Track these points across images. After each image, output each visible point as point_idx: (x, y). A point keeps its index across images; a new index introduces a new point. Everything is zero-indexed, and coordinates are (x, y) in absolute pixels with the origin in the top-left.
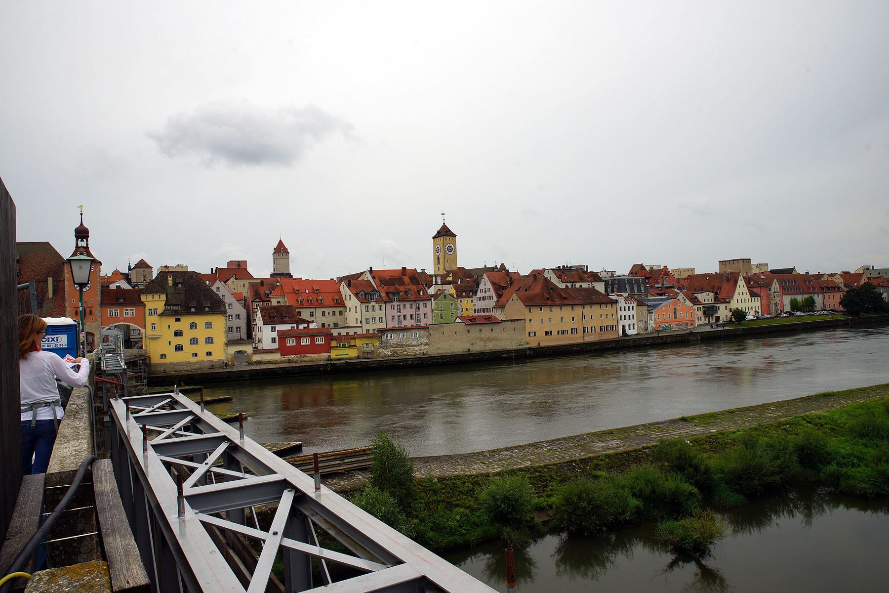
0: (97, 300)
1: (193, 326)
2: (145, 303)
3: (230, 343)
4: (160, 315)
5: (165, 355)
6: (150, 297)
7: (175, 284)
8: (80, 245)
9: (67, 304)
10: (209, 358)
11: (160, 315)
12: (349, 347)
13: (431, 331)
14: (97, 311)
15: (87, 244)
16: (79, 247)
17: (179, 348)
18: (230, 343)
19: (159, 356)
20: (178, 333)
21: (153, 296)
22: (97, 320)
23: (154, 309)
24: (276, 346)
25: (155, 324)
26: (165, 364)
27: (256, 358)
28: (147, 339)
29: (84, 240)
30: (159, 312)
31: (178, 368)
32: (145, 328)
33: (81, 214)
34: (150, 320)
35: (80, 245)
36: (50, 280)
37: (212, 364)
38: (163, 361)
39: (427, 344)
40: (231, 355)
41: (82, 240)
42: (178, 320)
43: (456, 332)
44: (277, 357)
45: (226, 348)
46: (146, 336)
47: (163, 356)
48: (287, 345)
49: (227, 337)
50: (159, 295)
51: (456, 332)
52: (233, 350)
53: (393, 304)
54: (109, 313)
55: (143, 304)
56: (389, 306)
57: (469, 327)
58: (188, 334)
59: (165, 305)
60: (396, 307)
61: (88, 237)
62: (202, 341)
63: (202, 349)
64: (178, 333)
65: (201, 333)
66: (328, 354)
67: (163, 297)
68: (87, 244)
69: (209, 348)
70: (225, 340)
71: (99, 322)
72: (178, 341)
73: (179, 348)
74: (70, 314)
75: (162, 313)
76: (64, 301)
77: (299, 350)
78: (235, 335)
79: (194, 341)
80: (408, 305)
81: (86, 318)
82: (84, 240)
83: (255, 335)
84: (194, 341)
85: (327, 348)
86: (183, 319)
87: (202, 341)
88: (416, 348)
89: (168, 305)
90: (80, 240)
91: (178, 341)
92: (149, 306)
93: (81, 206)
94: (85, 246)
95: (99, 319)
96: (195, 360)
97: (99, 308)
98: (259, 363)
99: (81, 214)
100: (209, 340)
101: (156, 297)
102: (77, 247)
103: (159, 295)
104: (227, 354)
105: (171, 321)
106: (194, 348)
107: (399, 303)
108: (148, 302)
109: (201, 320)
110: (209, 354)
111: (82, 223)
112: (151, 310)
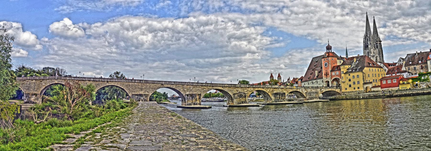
4: (344, 73)
10: (359, 90)
12: (407, 83)
14: (330, 74)
26: (347, 92)
27: (373, 90)
30: (344, 73)
34: (343, 75)
48: (383, 83)
62: (356, 83)
69: (358, 86)
95: (330, 76)
96: (354, 90)
98: (374, 91)
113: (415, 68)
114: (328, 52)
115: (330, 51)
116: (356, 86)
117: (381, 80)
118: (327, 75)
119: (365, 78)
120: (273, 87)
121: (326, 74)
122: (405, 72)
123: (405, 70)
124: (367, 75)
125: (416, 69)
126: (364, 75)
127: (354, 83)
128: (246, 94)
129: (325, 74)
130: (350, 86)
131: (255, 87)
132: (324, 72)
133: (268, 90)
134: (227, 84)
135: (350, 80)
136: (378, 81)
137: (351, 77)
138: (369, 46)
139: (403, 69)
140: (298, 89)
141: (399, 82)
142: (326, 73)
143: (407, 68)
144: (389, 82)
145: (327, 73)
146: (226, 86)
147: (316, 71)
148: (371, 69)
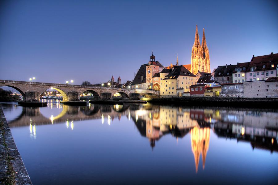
13: (245, 86)
14: (152, 80)
24: (189, 90)
26: (164, 95)
31: (166, 97)
38: (163, 94)
39: (243, 92)
43: (259, 86)
44: (189, 95)
51: (259, 86)
53: (251, 72)
56: (248, 74)
57: (268, 83)
60: (253, 74)
62: (171, 88)
66: (204, 95)
77: (195, 92)
80: (260, 73)
85: (203, 92)
88: (237, 94)
96: (169, 94)
97: (152, 78)
107: (254, 72)
113: (223, 79)
114: (152, 61)
115: (154, 61)
117: (191, 88)
119: (178, 85)
120: (102, 88)
122: (213, 81)
123: (214, 80)
124: (180, 83)
125: (224, 79)
126: (178, 82)
127: (170, 88)
128: (78, 93)
130: (167, 91)
131: (86, 88)
133: (98, 90)
134: (63, 84)
135: (167, 86)
136: (188, 88)
139: (212, 79)
140: (123, 90)
141: (205, 91)
143: (215, 78)
144: (197, 89)
146: (61, 86)
148: (185, 77)
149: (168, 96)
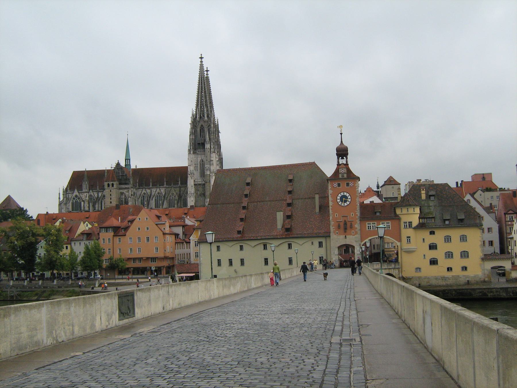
0: (357, 213)
1: (448, 239)
2: (400, 216)
3: (486, 258)
4: (415, 228)
5: (420, 269)
6: (405, 211)
7: (429, 197)
8: (340, 163)
9: (331, 218)
10: (465, 273)
11: (415, 228)
14: (357, 226)
15: (347, 162)
16: (340, 165)
17: (434, 262)
18: (486, 258)
19: (414, 270)
20: (433, 247)
21: (408, 209)
22: (356, 233)
23: (409, 222)
25: (409, 237)
26: (419, 278)
28: (402, 252)
29: (344, 158)
32: (400, 240)
33: (341, 134)
34: (406, 232)
35: (340, 163)
36: (317, 197)
37: (467, 279)
38: (418, 274)
40: (487, 270)
41: (343, 158)
42: (432, 233)
45: (482, 263)
46: (401, 249)
47: (418, 269)
49: (483, 251)
50: (414, 208)
52: (489, 265)
54: (367, 226)
55: (397, 218)
58: (443, 248)
59: (419, 218)
61: (347, 154)
62: (457, 255)
63: (457, 263)
64: (433, 247)
65: (456, 247)
67: (417, 210)
68: (347, 162)
69: (465, 262)
70: (480, 255)
71: (358, 236)
72: (433, 254)
73: (434, 262)
74: (334, 227)
75: (417, 226)
76: (329, 216)
78: (490, 250)
79: (449, 255)
81: (348, 231)
82: (344, 158)
83: (511, 250)
84: (449, 255)
86: (437, 232)
87: (457, 255)
89: (422, 218)
90: (341, 158)
91: (433, 254)
92: (405, 219)
93: (341, 127)
94: (345, 163)
95: (359, 232)
96: (449, 274)
97: (358, 222)
99: (341, 134)
100: (465, 254)
101: (411, 210)
102: (339, 165)
103: (414, 208)
104: (484, 270)
105: (425, 234)
106: (449, 263)
108: (402, 215)
109: (455, 234)
110: (465, 268)
111: (342, 142)
112: (406, 223)
116: (457, 263)
118: (345, 229)
121: (342, 224)
129: (339, 227)
132: (334, 216)
137: (439, 237)
138: (207, 146)
142: (345, 224)
145: (348, 224)
147: (278, 213)
149: (444, 278)
